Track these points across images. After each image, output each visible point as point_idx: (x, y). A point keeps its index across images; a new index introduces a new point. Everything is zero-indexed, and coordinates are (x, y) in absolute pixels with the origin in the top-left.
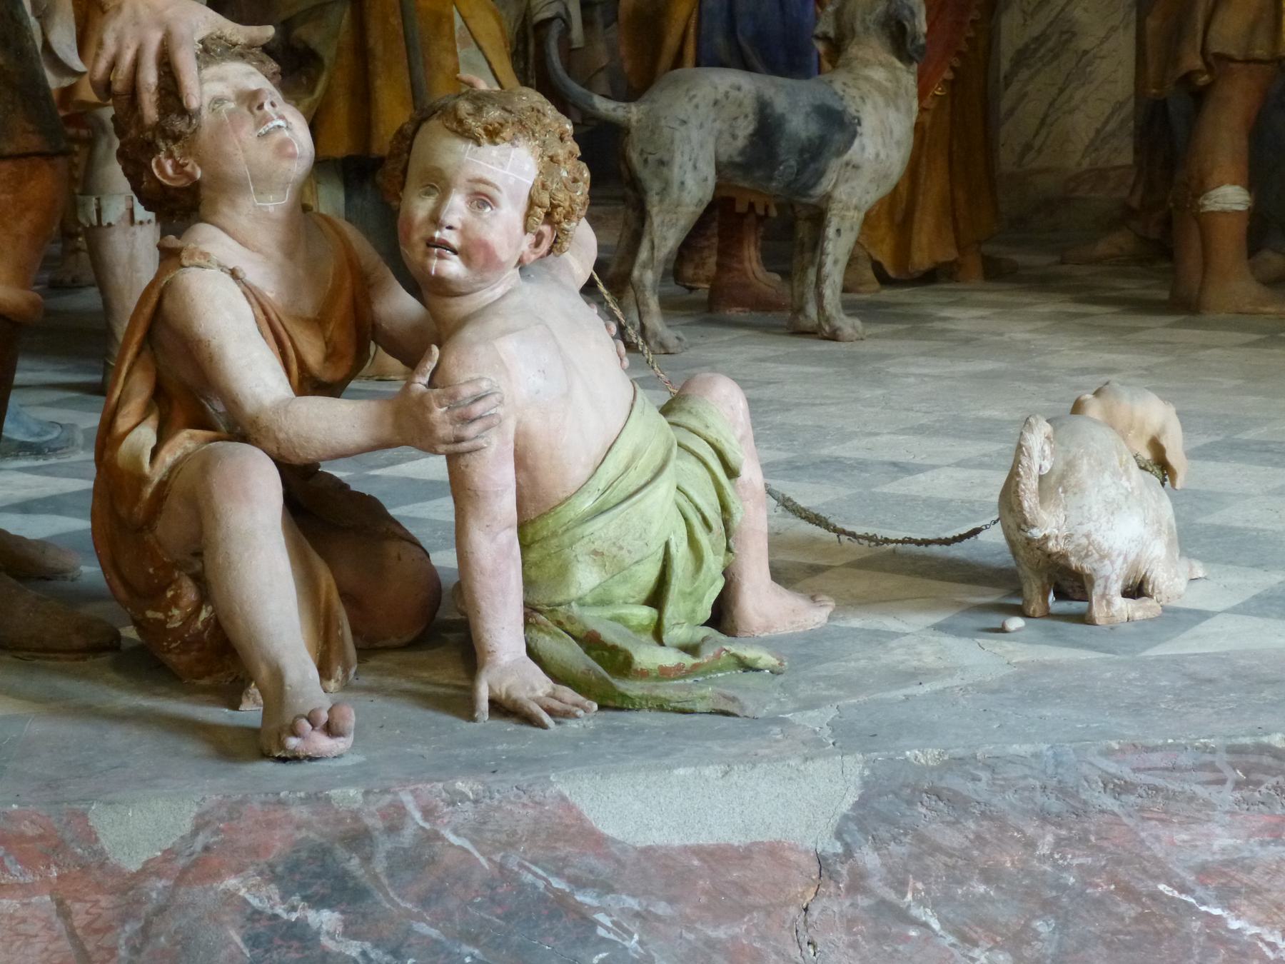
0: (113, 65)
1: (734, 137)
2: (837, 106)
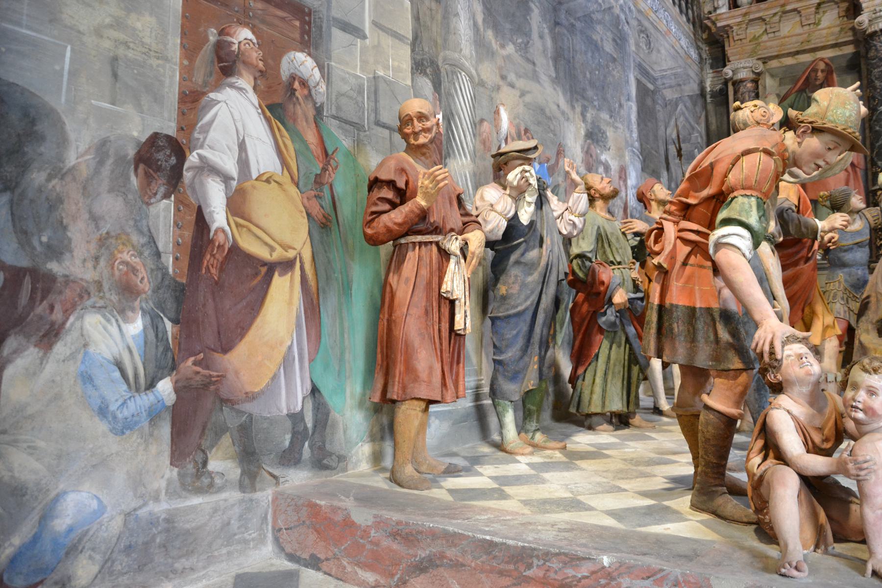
0: (757, 345)
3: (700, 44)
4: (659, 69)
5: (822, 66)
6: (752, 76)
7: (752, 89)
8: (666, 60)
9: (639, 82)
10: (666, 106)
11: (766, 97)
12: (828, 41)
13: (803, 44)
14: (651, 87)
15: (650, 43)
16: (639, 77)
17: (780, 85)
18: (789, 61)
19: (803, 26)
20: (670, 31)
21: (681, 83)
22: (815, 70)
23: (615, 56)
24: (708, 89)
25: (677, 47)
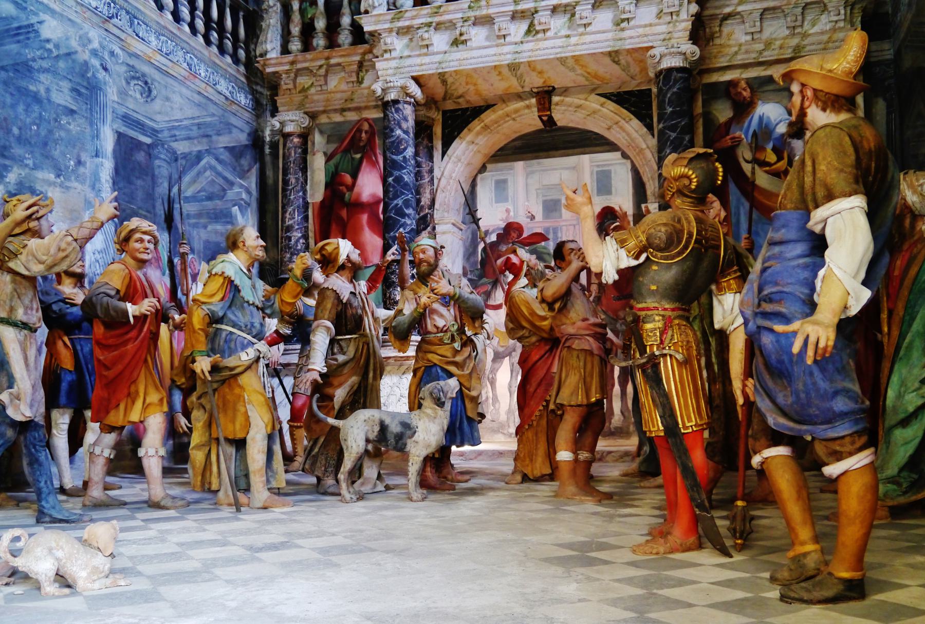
1: (373, 432)
2: (409, 422)
3: (259, 88)
4: (167, 119)
5: (366, 126)
8: (181, 109)
9: (120, 136)
10: (176, 160)
11: (314, 155)
12: (369, 101)
13: (347, 102)
14: (147, 140)
15: (150, 91)
16: (123, 129)
17: (328, 142)
18: (337, 118)
19: (347, 82)
20: (195, 75)
21: (210, 133)
22: (359, 131)
23: (74, 108)
24: (268, 139)
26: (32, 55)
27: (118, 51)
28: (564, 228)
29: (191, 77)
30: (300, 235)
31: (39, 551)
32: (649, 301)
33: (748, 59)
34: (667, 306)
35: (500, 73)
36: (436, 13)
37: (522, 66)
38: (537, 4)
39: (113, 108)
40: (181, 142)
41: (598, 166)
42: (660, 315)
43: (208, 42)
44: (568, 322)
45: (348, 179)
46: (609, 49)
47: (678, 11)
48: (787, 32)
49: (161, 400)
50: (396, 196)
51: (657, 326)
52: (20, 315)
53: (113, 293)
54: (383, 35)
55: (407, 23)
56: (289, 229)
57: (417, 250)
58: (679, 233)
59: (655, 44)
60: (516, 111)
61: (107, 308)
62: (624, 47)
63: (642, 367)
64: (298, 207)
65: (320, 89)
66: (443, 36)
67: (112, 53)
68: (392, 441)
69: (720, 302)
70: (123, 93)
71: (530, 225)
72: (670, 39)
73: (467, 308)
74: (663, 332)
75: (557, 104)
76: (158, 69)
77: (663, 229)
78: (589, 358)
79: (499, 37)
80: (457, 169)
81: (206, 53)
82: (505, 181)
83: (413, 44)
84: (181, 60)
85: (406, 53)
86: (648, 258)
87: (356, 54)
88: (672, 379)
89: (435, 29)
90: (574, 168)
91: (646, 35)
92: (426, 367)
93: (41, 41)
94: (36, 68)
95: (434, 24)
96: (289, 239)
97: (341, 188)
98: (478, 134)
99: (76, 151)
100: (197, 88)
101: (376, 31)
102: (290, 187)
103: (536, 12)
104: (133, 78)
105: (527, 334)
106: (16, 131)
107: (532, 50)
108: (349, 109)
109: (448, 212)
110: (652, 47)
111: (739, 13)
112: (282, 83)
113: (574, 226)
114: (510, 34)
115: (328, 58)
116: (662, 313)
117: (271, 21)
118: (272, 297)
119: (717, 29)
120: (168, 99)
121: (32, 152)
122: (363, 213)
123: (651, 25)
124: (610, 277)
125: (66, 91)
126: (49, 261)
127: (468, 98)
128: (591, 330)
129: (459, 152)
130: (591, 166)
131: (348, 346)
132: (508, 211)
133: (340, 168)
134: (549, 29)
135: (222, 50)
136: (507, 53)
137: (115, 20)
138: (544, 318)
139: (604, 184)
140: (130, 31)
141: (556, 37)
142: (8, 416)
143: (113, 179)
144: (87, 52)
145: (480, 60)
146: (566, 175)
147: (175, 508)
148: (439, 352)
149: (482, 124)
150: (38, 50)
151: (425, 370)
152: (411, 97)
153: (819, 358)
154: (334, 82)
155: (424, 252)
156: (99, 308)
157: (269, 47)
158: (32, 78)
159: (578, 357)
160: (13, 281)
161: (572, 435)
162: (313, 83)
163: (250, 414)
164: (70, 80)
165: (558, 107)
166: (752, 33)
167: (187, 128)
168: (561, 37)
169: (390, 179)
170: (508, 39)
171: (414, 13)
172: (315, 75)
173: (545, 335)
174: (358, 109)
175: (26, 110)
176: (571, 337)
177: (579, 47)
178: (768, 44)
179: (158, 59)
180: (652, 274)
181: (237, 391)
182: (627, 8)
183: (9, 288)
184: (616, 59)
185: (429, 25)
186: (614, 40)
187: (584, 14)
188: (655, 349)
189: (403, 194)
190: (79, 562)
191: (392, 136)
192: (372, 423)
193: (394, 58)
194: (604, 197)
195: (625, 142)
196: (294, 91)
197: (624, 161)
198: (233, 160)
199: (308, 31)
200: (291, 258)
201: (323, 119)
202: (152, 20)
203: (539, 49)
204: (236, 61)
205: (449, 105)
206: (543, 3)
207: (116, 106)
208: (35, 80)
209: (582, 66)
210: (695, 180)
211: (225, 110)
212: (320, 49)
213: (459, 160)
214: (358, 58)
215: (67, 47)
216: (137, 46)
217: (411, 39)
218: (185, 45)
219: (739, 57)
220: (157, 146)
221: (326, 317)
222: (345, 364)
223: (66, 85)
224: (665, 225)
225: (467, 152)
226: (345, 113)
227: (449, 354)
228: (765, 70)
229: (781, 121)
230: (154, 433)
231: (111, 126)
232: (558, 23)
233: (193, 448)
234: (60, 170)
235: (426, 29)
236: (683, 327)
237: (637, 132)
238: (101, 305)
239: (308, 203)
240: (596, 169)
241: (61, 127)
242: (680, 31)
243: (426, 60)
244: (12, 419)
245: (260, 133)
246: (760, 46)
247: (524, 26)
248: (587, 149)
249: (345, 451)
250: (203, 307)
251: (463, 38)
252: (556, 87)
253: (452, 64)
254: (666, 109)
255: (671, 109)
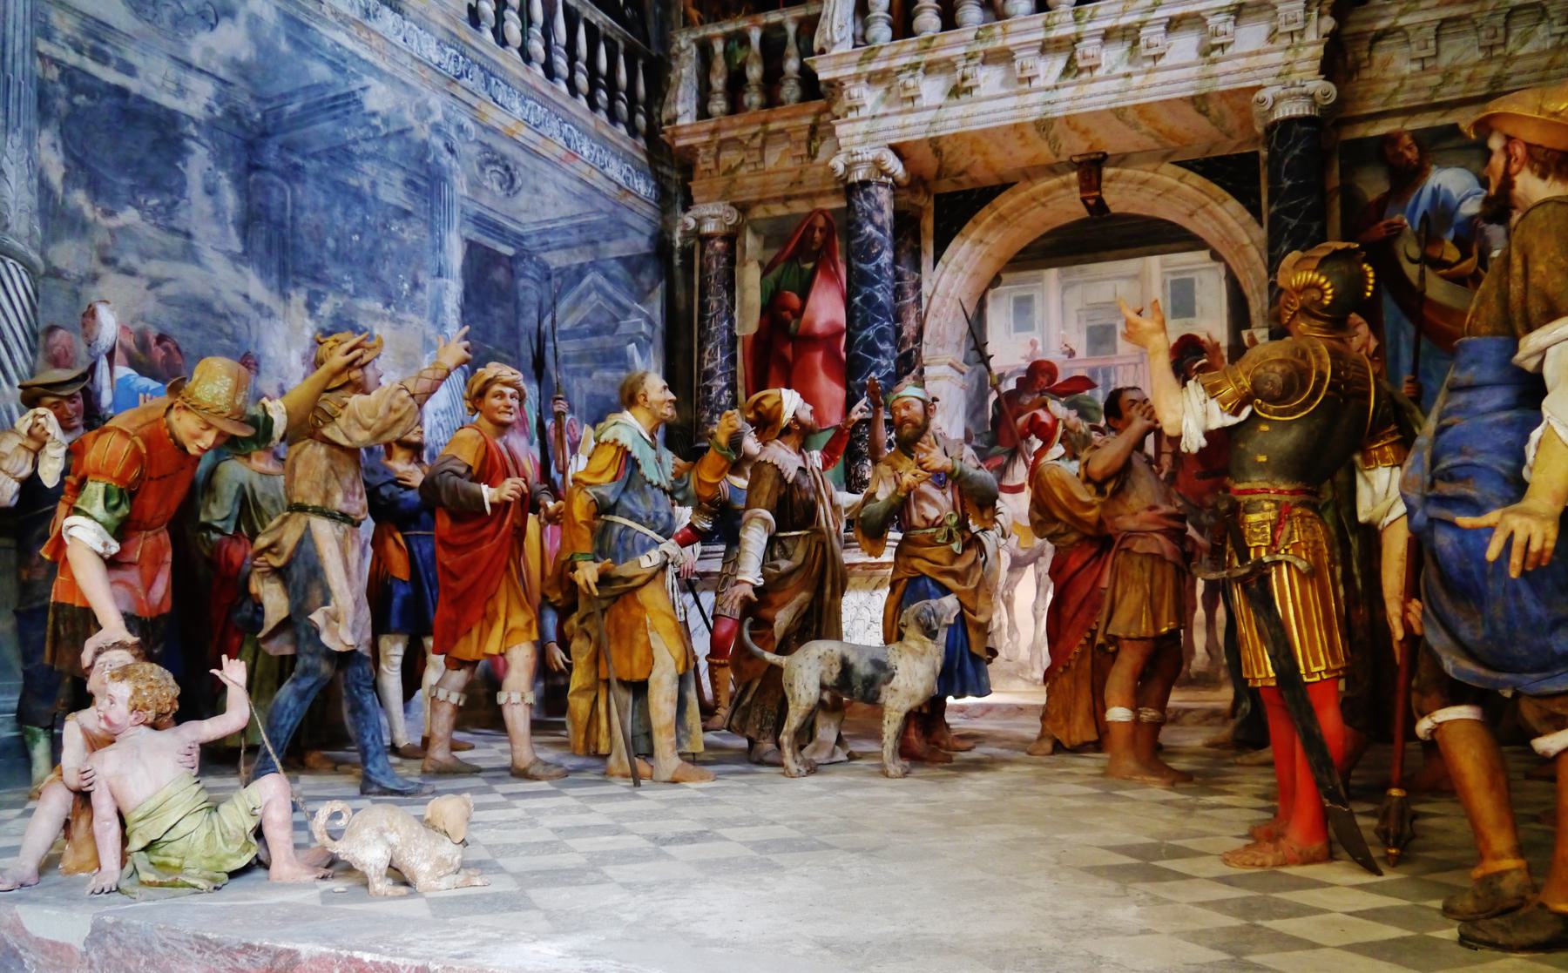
2: (884, 660)
3: (665, 170)
4: (536, 219)
5: (821, 222)
6: (721, 230)
7: (722, 252)
8: (556, 205)
9: (472, 247)
10: (549, 278)
14: (509, 251)
15: (512, 179)
16: (475, 236)
17: (766, 246)
18: (779, 210)
21: (596, 238)
22: (811, 228)
23: (409, 208)
24: (678, 244)
25: (596, 179)
26: (353, 135)
27: (468, 124)
28: (1120, 369)
29: (570, 157)
30: (724, 384)
31: (367, 833)
32: (1254, 479)
33: (1415, 100)
34: (1283, 487)
35: (1022, 136)
36: (926, 48)
37: (1056, 124)
38: (1080, 28)
39: (463, 207)
40: (555, 252)
41: (1174, 273)
42: (1272, 501)
43: (593, 106)
44: (1126, 511)
45: (794, 300)
46: (1192, 93)
47: (1303, 30)
48: (1480, 55)
49: (529, 624)
50: (865, 325)
51: (1267, 518)
52: (338, 502)
53: (463, 470)
54: (847, 85)
55: (882, 66)
56: (709, 375)
57: (897, 404)
58: (1304, 374)
59: (1265, 82)
60: (1047, 192)
61: (454, 491)
62: (1215, 89)
63: (1243, 581)
64: (722, 342)
65: (752, 167)
66: (936, 83)
67: (460, 128)
68: (859, 687)
69: (1367, 480)
70: (475, 185)
71: (1067, 366)
72: (1289, 73)
73: (973, 490)
74: (1276, 527)
75: (1110, 180)
76: (524, 147)
77: (1278, 369)
78: (1158, 567)
79: (1021, 81)
80: (956, 282)
81: (591, 122)
82: (1029, 299)
83: (892, 96)
84: (556, 133)
85: (881, 110)
86: (1253, 413)
87: (806, 115)
88: (1289, 599)
89: (926, 72)
90: (1135, 277)
91: (1251, 69)
92: (909, 578)
93: (364, 115)
94: (358, 152)
95: (923, 65)
96: (709, 390)
97: (784, 313)
98: (989, 228)
99: (411, 269)
100: (578, 174)
101: (835, 80)
102: (710, 314)
103: (1079, 40)
104: (489, 162)
105: (1062, 530)
106: (331, 243)
107: (1072, 99)
108: (796, 197)
109: (943, 346)
110: (1260, 87)
111: (1401, 29)
112: (699, 161)
113: (1136, 365)
114: (1037, 76)
115: (765, 123)
116: (1275, 497)
117: (684, 71)
118: (686, 474)
119: (1365, 55)
120: (537, 190)
121: (352, 273)
122: (818, 350)
123: (1258, 53)
124: (1194, 441)
125: (399, 184)
126: (378, 426)
127: (973, 174)
128: (1162, 524)
129: (959, 256)
130: (1163, 273)
131: (795, 547)
132: (1033, 344)
133: (782, 286)
134: (1098, 66)
135: (613, 117)
136: (1034, 105)
137: (465, 81)
138: (1089, 506)
139: (1183, 299)
140: (485, 95)
141: (1109, 77)
142: (322, 645)
143: (461, 307)
144: (426, 127)
145: (993, 116)
146: (1123, 287)
147: (548, 778)
148: (930, 556)
149: (995, 214)
150: (361, 127)
151: (907, 583)
152: (888, 175)
153: (1529, 569)
154: (773, 158)
155: (907, 407)
156: (443, 491)
157: (680, 108)
158: (353, 168)
159: (1141, 564)
160: (329, 455)
161: (1130, 683)
162: (743, 161)
163: (653, 644)
164: (404, 168)
165: (1112, 185)
166: (1422, 59)
167: (565, 232)
168: (1117, 77)
169: (857, 299)
170: (1035, 83)
171: (894, 50)
172: (746, 148)
173: (1090, 531)
174: (810, 196)
175: (345, 214)
176: (1131, 534)
177: (1145, 92)
178: (1448, 76)
179: (524, 134)
180: (1259, 437)
181: (635, 611)
182: (1221, 28)
183: (323, 464)
184: (1204, 108)
185: (915, 66)
186: (1200, 78)
187: (1154, 40)
188: (1263, 553)
189: (877, 320)
190: (420, 850)
191: (860, 235)
192: (829, 661)
193: (863, 119)
194: (1183, 320)
195: (1216, 235)
196: (715, 173)
197: (1214, 264)
198: (629, 276)
199: (736, 83)
200: (711, 418)
201: (758, 213)
202: (515, 77)
203: (1083, 97)
204: (633, 131)
205: (946, 186)
206: (1090, 27)
207: (466, 203)
208: (357, 171)
209: (1151, 120)
210: (1330, 292)
211: (617, 204)
212: (754, 109)
213: (961, 269)
214: (808, 121)
215: (401, 122)
216: (495, 117)
217: (888, 90)
218: (561, 112)
219: (1401, 97)
220: (521, 258)
221: (763, 504)
222: (790, 573)
223: (397, 176)
224: (1281, 361)
225: (972, 256)
226: (789, 203)
227: (944, 560)
228: (1443, 116)
229: (1468, 196)
230: (519, 671)
231: (459, 232)
232: (1113, 57)
233: (572, 694)
234: (390, 296)
235: (910, 73)
236: (1308, 520)
237: (1235, 218)
238: (447, 488)
239: (736, 337)
240: (1170, 278)
241: (391, 236)
242: (1306, 60)
243: (911, 119)
244: (328, 649)
245: (668, 236)
246: (1435, 79)
247: (1060, 62)
248: (1158, 248)
249: (790, 702)
250: (588, 490)
251: (966, 84)
252: (1109, 153)
253: (950, 123)
254: (1281, 183)
255: (1289, 183)
